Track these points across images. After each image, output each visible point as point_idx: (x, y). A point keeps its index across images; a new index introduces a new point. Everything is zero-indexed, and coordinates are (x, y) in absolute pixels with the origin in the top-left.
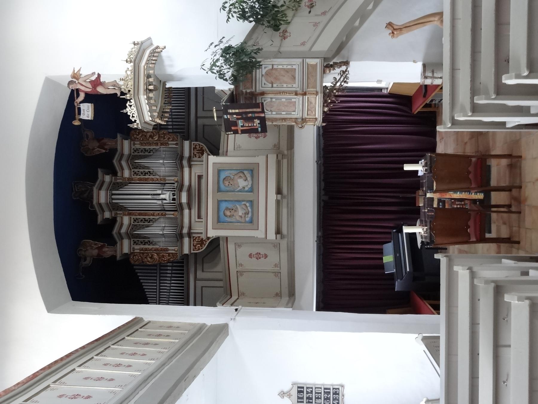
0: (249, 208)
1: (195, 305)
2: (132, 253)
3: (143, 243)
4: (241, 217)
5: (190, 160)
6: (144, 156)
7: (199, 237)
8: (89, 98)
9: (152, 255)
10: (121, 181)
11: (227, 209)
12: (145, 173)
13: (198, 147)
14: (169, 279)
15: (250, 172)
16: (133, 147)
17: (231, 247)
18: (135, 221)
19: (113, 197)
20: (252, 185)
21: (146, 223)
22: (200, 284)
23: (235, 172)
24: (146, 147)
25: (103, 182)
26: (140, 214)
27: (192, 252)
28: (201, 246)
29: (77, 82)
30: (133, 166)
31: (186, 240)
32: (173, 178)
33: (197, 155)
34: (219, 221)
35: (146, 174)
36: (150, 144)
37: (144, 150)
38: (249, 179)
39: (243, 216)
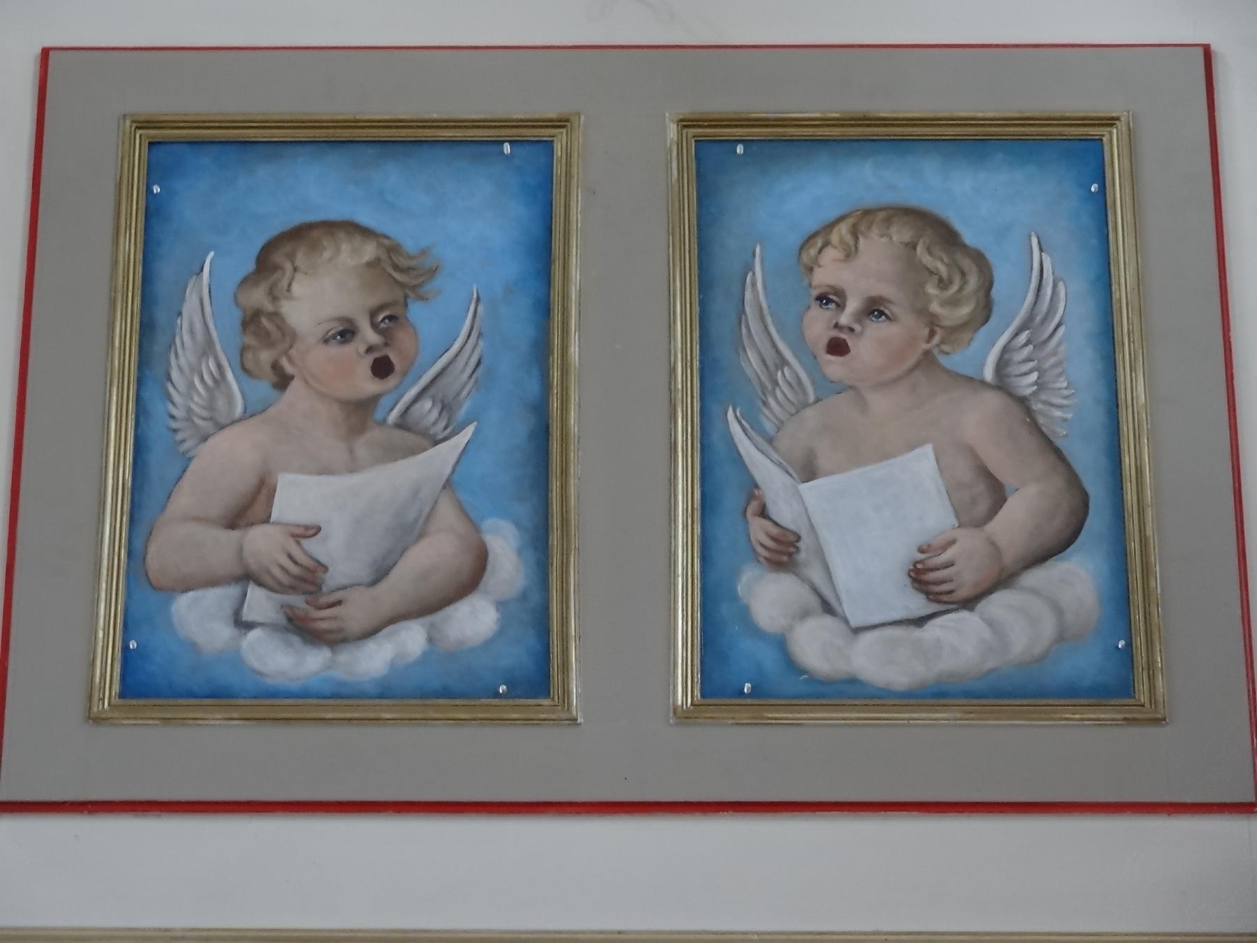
0: (411, 639)
4: (249, 508)
11: (401, 279)
15: (1087, 663)
20: (846, 693)
23: (1070, 407)
38: (960, 641)
39: (262, 543)
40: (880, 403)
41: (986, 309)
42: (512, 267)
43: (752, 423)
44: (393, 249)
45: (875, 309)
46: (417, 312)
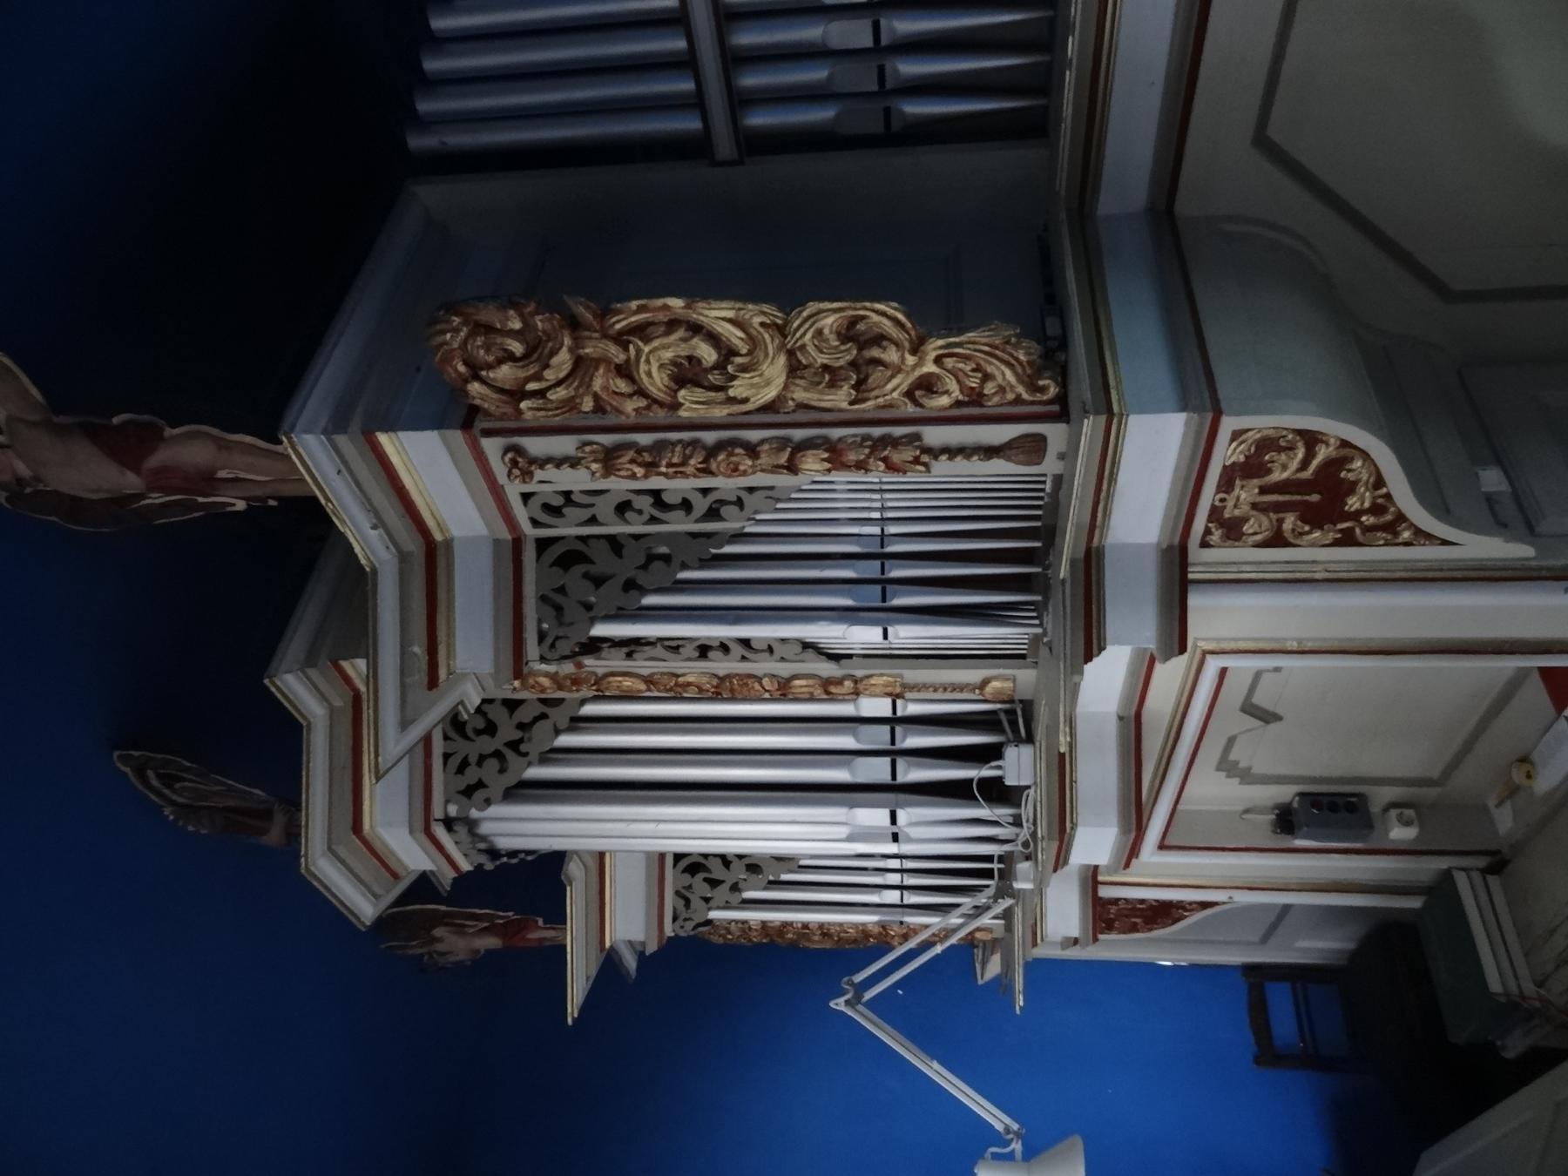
5: (1177, 579)
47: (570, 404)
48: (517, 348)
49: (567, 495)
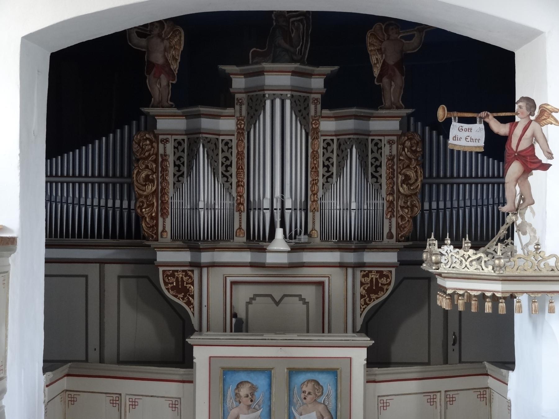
1: (48, 261)
2: (156, 136)
3: (178, 163)
6: (366, 166)
7: (192, 283)
8: (496, 146)
9: (152, 181)
10: (312, 113)
11: (254, 389)
12: (328, 167)
13: (384, 280)
14: (103, 203)
16: (385, 139)
17: (172, 389)
18: (227, 144)
19: (278, 102)
21: (221, 169)
22: (93, 271)
23: (331, 407)
24: (384, 167)
25: (309, 75)
26: (240, 155)
27: (161, 269)
28: (173, 288)
29: (532, 118)
30: (343, 143)
31: (185, 256)
32: (317, 227)
33: (368, 280)
34: (227, 371)
35: (327, 167)
36: (391, 177)
37: (378, 163)
40: (310, 406)
41: (322, 393)
42: (266, 387)
43: (295, 408)
44: (253, 385)
45: (309, 393)
46: (256, 393)
47: (401, 155)
48: (414, 149)
49: (381, 148)
